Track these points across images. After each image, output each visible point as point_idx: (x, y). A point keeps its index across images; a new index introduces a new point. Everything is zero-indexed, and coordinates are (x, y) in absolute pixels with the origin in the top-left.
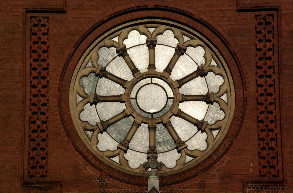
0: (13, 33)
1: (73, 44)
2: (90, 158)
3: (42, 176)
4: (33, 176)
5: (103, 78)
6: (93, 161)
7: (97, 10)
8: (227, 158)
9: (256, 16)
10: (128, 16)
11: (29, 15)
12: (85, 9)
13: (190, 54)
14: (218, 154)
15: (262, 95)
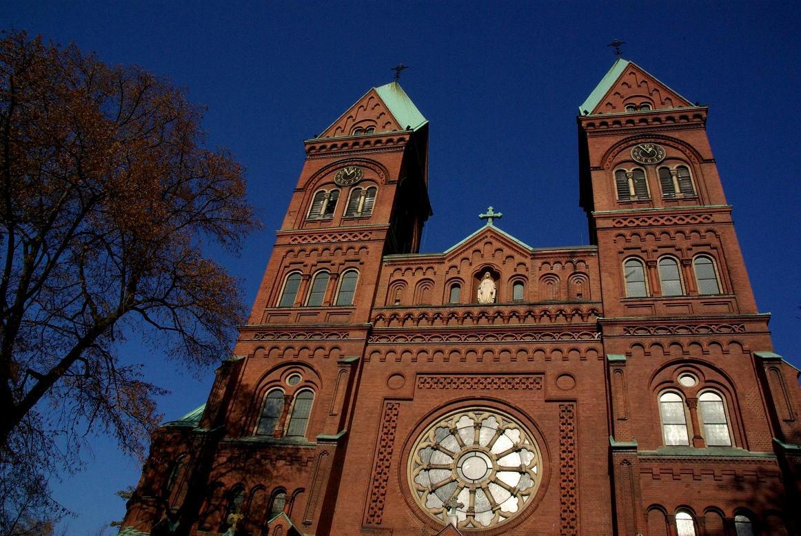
0: (372, 414)
1: (415, 423)
2: (418, 512)
3: (377, 523)
4: (370, 523)
5: (437, 451)
6: (420, 515)
7: (436, 398)
8: (532, 518)
9: (560, 406)
10: (460, 404)
11: (386, 402)
12: (428, 398)
13: (507, 434)
14: (525, 515)
15: (564, 466)
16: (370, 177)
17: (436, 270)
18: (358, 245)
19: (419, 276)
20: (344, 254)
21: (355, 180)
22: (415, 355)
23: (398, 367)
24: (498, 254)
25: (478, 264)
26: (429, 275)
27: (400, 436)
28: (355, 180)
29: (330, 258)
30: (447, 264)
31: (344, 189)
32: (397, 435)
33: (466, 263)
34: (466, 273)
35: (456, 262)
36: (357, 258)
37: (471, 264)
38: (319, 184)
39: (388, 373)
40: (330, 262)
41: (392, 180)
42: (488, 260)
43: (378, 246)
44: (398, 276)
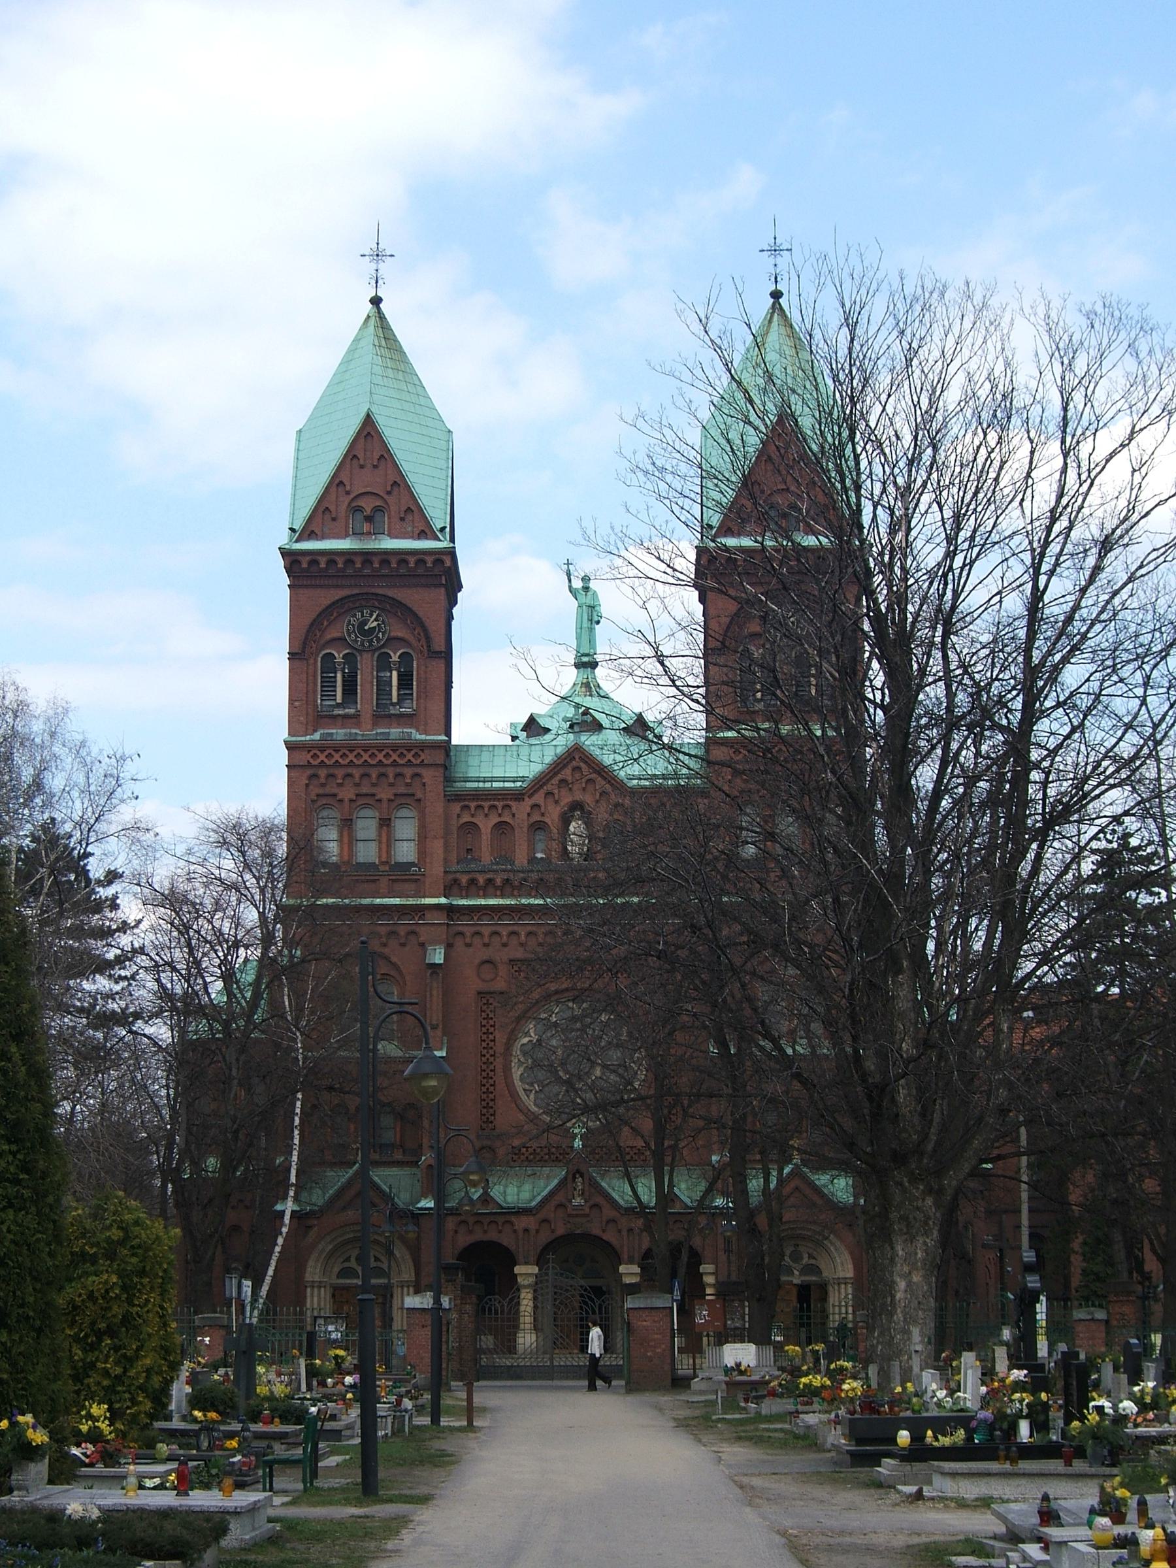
16: (400, 634)
17: (514, 809)
18: (409, 772)
19: (494, 819)
20: (391, 785)
21: (379, 640)
22: (505, 939)
23: (484, 954)
24: (590, 787)
25: (567, 799)
26: (507, 818)
27: (500, 1037)
28: (379, 640)
29: (373, 790)
30: (528, 802)
31: (365, 655)
32: (498, 1035)
33: (550, 800)
34: (553, 815)
35: (539, 798)
36: (410, 792)
37: (557, 802)
38: (322, 642)
39: (477, 961)
40: (374, 795)
41: (437, 649)
42: (578, 796)
43: (437, 774)
44: (466, 818)
